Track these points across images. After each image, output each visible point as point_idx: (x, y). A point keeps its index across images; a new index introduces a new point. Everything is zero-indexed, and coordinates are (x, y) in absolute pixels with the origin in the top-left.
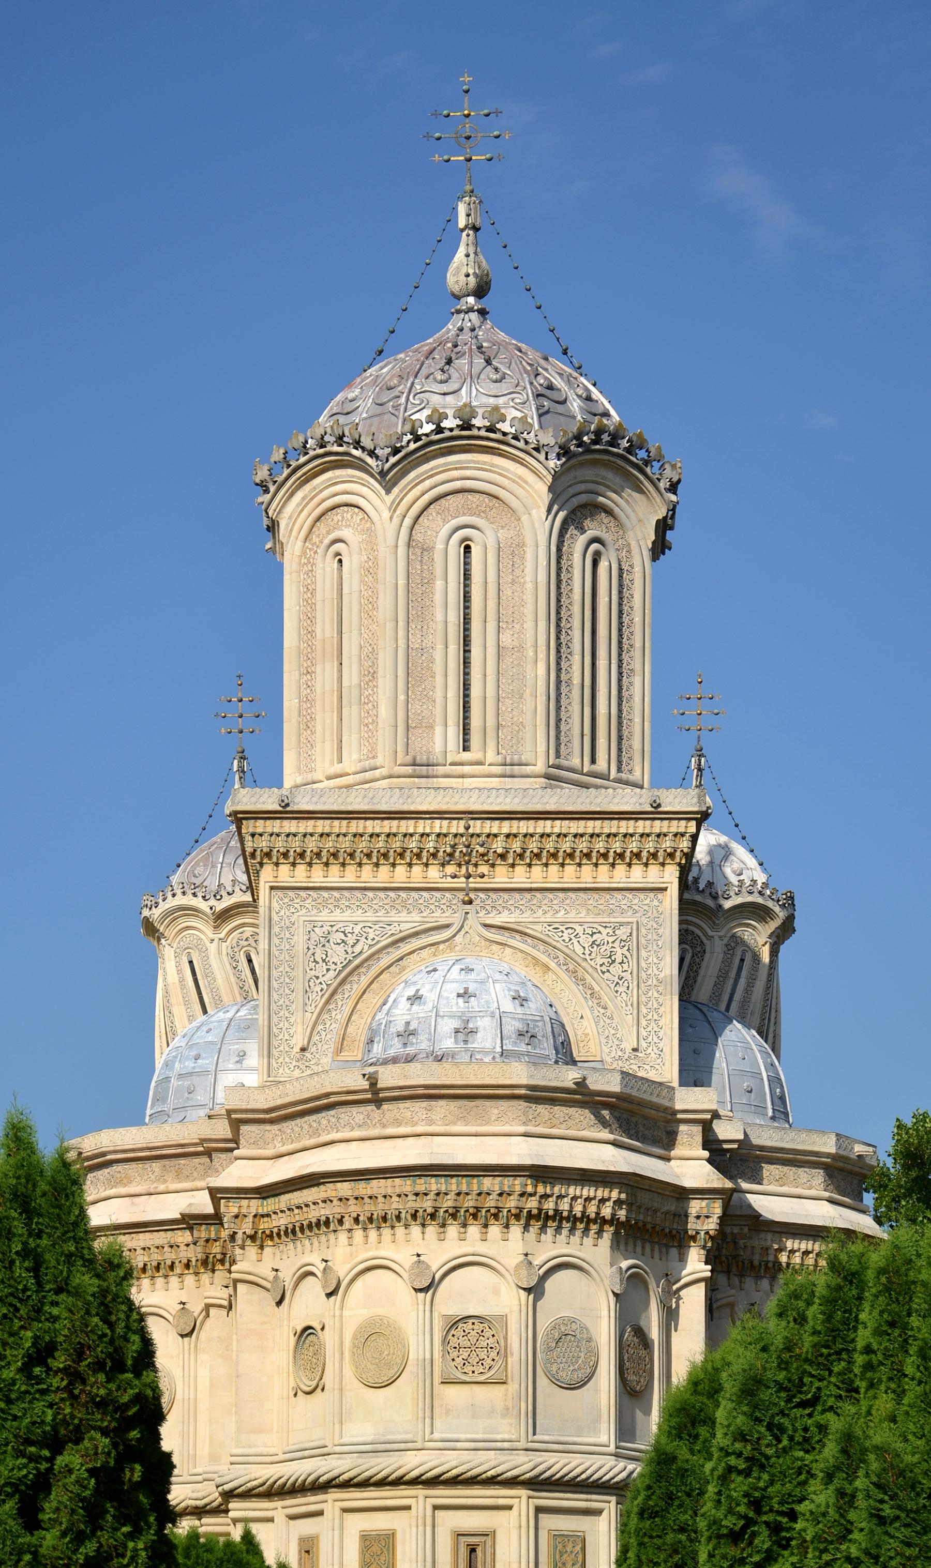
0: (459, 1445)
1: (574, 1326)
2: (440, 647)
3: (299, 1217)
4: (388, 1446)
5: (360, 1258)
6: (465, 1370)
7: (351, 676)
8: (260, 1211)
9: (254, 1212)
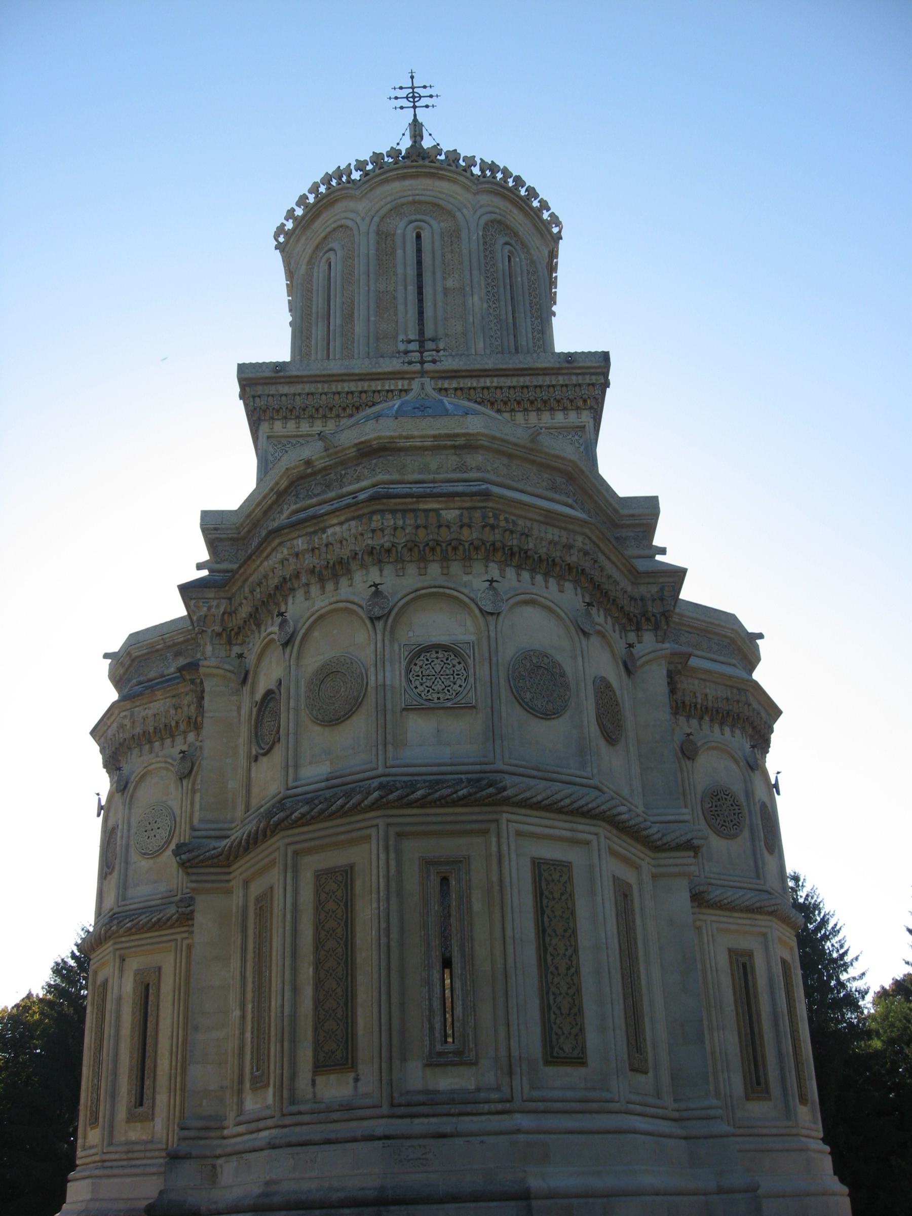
1: (546, 660)
2: (400, 288)
6: (430, 697)
8: (229, 610)
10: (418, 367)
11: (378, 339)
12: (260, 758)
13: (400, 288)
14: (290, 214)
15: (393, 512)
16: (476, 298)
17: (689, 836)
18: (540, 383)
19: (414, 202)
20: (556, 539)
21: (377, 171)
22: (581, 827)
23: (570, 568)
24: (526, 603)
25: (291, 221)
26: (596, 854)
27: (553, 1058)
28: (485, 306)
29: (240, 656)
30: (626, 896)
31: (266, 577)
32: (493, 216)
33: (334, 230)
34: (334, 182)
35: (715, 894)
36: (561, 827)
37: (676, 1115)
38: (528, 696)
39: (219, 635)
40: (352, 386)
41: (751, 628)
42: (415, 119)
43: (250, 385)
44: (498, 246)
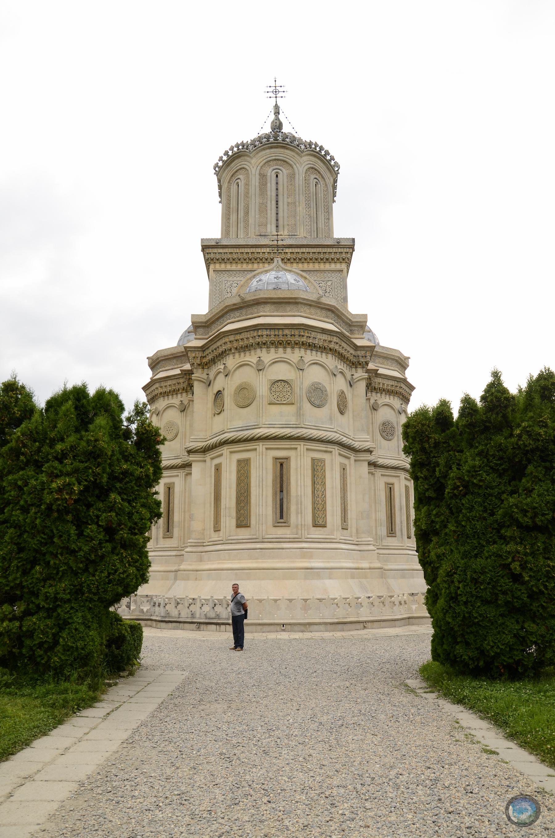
0: (276, 426)
1: (320, 386)
3: (216, 353)
4: (248, 428)
5: (238, 362)
7: (241, 214)
9: (200, 355)
10: (275, 243)
11: (259, 226)
12: (216, 415)
13: (269, 202)
14: (221, 159)
15: (266, 329)
16: (301, 209)
17: (369, 447)
18: (325, 251)
19: (275, 160)
20: (326, 339)
21: (260, 145)
22: (329, 446)
23: (331, 349)
24: (314, 364)
25: (221, 162)
26: (334, 456)
27: (315, 525)
28: (305, 211)
29: (208, 374)
30: (344, 469)
31: (218, 347)
32: (310, 166)
33: (240, 169)
34: (240, 147)
35: (381, 461)
36: (322, 447)
37: (357, 543)
38: (313, 399)
39: (199, 365)
40: (248, 250)
41: (406, 355)
42: (276, 104)
43: (206, 248)
44: (311, 181)
